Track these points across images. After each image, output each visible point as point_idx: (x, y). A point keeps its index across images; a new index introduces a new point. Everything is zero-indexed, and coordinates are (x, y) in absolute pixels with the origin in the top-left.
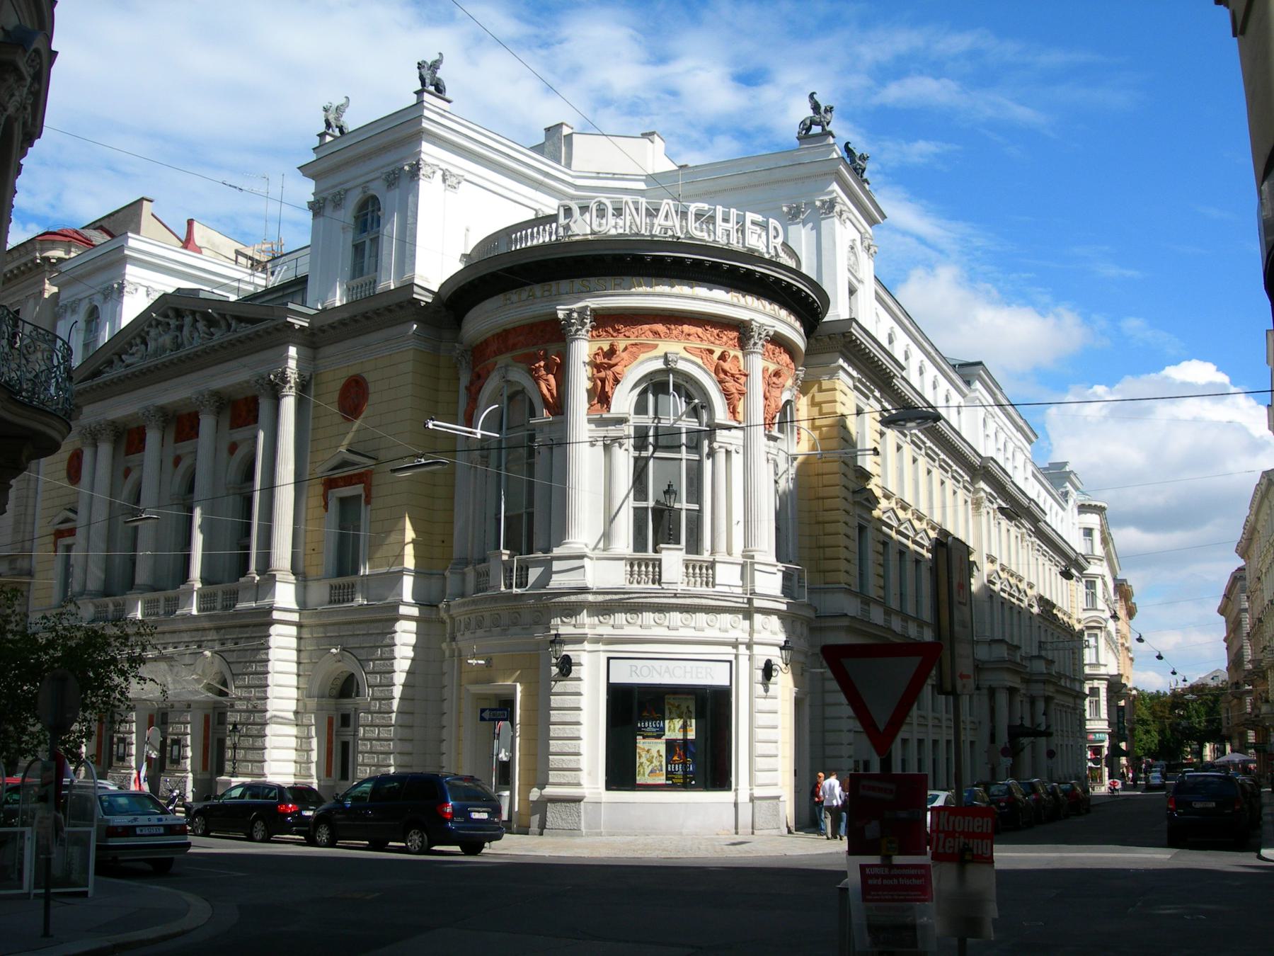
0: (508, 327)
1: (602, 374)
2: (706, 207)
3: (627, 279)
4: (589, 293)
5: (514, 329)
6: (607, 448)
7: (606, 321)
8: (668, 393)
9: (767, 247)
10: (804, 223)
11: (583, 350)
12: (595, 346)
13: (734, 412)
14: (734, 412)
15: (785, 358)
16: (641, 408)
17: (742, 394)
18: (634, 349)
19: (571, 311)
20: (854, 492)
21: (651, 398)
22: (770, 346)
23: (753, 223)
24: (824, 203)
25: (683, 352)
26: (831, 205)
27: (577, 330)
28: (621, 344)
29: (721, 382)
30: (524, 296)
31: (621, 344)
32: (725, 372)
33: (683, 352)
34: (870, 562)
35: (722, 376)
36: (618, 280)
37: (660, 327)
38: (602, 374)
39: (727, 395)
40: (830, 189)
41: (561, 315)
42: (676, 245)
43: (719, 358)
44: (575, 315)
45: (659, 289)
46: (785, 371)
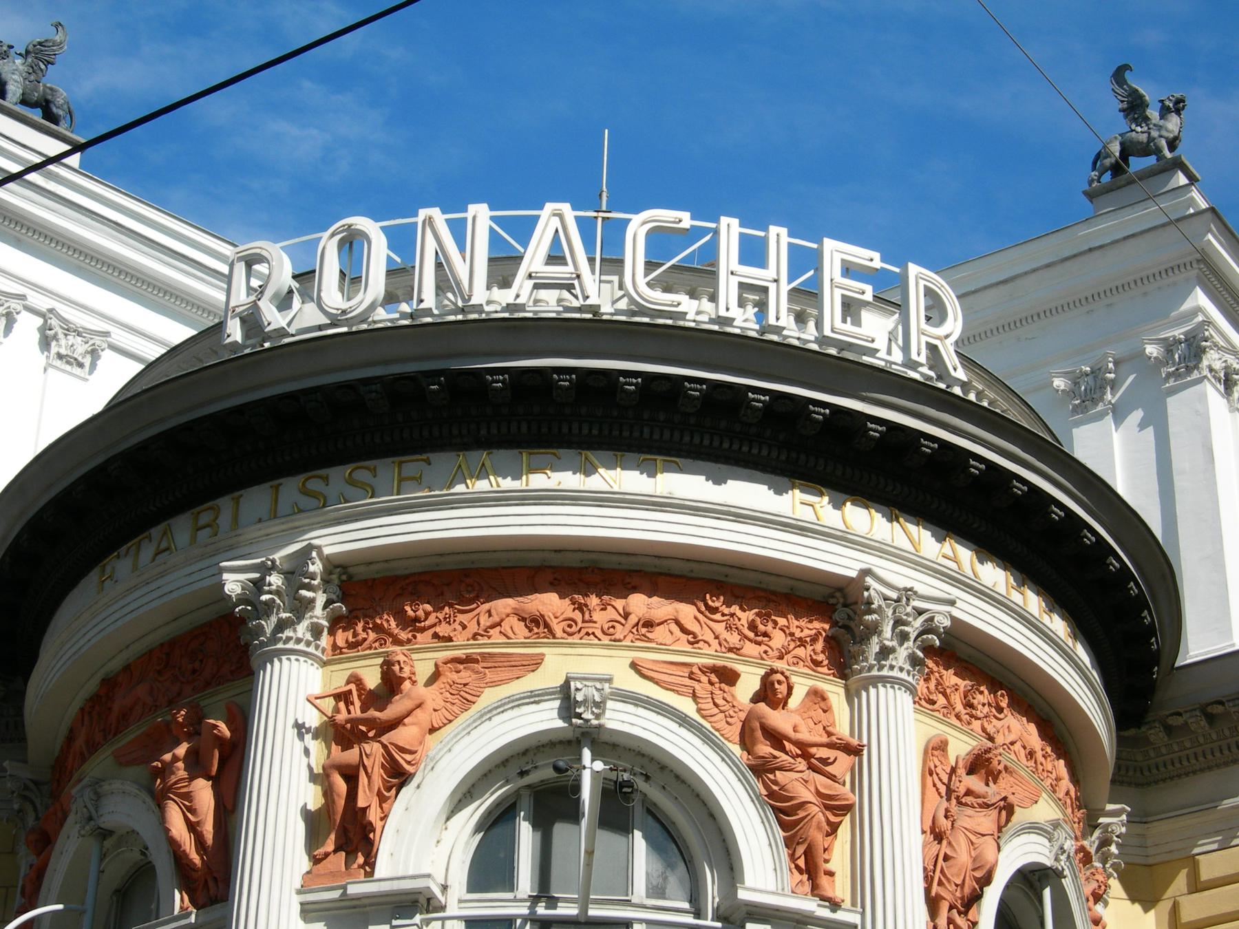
0: (116, 664)
1: (352, 756)
2: (686, 220)
3: (443, 461)
4: (321, 510)
5: (127, 668)
7: (376, 594)
8: (573, 814)
9: (906, 348)
10: (1119, 414)
11: (296, 689)
12: (338, 679)
13: (810, 868)
14: (810, 868)
15: (1018, 731)
16: (490, 869)
17: (838, 808)
18: (465, 675)
19: (265, 569)
21: (526, 835)
22: (950, 678)
23: (849, 270)
24: (1169, 346)
25: (630, 680)
26: (1190, 351)
27: (281, 626)
28: (420, 662)
29: (761, 769)
30: (147, 551)
31: (420, 662)
32: (776, 738)
33: (630, 680)
35: (765, 749)
36: (412, 466)
37: (550, 603)
38: (352, 756)
39: (783, 811)
40: (1187, 305)
41: (233, 584)
42: (590, 330)
43: (757, 698)
44: (275, 580)
45: (538, 481)
46: (1014, 758)
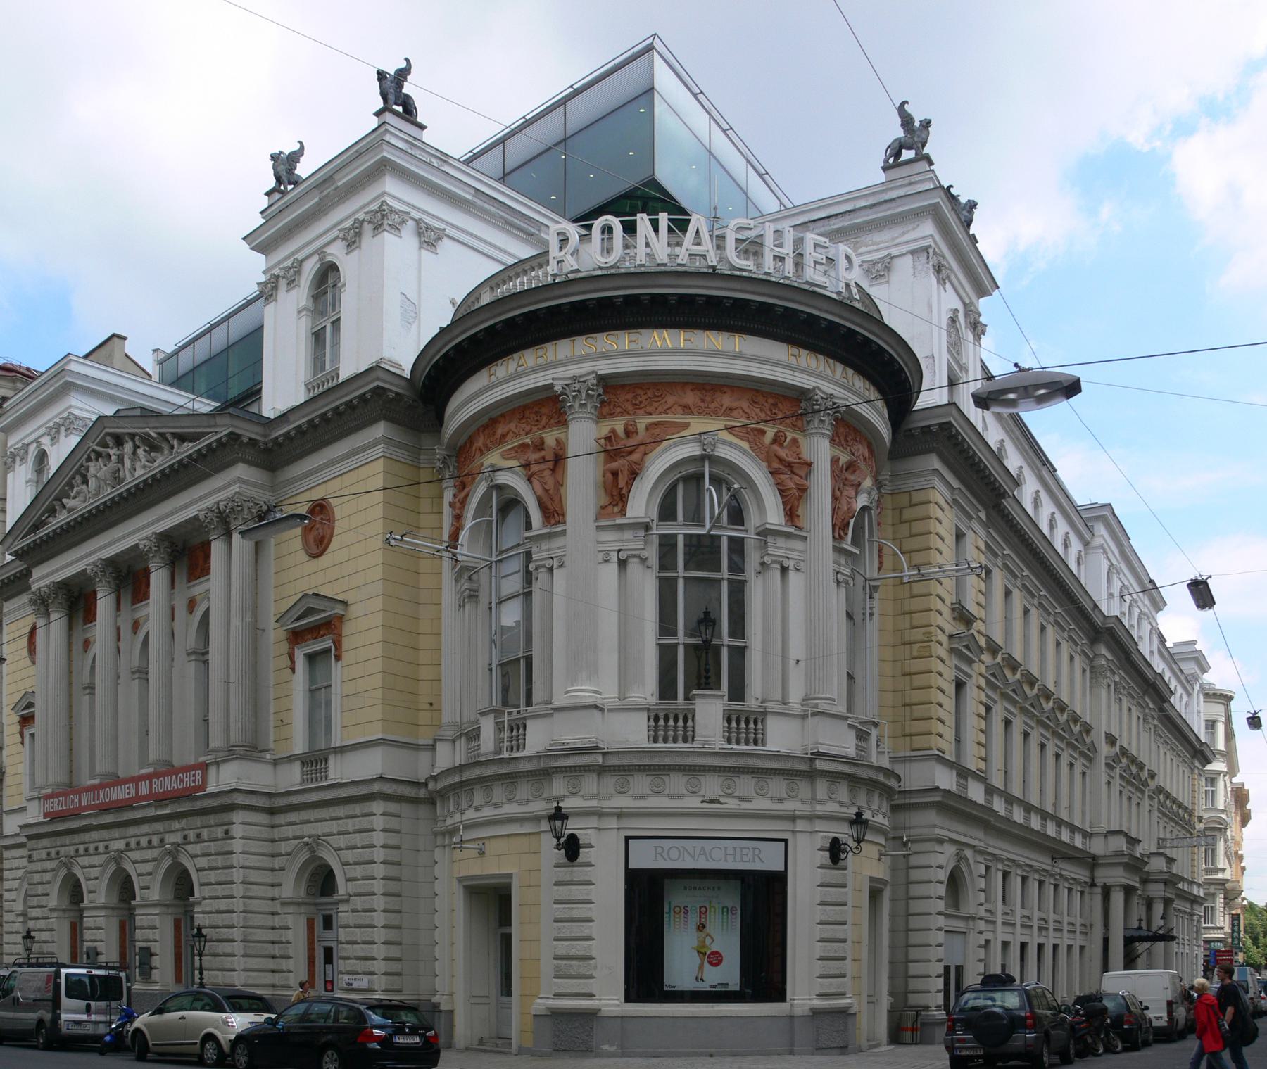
1: (614, 465)
6: (622, 564)
12: (605, 429)
15: (863, 450)
20: (951, 637)
28: (642, 422)
34: (969, 728)
38: (614, 465)
46: (861, 464)
